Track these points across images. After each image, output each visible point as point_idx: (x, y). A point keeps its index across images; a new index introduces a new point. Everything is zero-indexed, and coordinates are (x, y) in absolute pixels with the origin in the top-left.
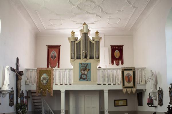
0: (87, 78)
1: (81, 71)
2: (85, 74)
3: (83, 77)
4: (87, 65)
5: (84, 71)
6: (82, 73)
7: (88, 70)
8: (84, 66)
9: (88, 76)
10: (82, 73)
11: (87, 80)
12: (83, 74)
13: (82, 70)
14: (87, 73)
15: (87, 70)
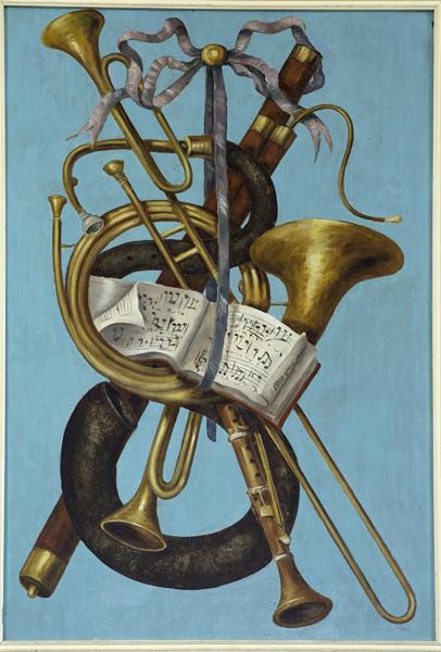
0: (306, 542)
1: (78, 309)
2: (211, 404)
3: (160, 488)
4: (301, 74)
5: (189, 308)
6: (103, 345)
7: (316, 266)
8: (186, 112)
9: (309, 460)
10: (103, 345)
11: (302, 611)
12: (149, 385)
13: (115, 263)
14: (296, 384)
15: (286, 264)
